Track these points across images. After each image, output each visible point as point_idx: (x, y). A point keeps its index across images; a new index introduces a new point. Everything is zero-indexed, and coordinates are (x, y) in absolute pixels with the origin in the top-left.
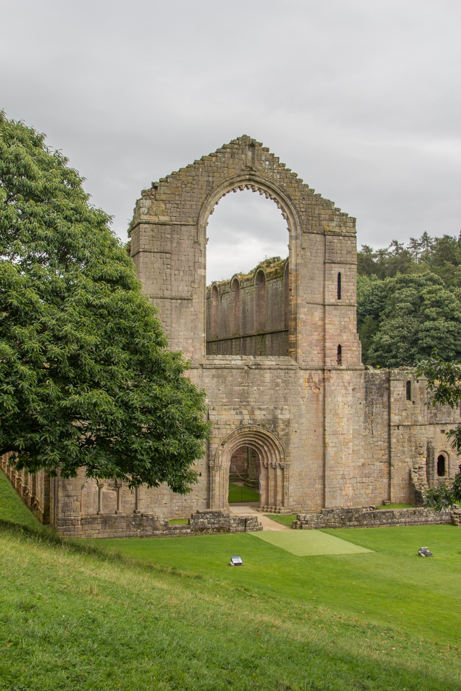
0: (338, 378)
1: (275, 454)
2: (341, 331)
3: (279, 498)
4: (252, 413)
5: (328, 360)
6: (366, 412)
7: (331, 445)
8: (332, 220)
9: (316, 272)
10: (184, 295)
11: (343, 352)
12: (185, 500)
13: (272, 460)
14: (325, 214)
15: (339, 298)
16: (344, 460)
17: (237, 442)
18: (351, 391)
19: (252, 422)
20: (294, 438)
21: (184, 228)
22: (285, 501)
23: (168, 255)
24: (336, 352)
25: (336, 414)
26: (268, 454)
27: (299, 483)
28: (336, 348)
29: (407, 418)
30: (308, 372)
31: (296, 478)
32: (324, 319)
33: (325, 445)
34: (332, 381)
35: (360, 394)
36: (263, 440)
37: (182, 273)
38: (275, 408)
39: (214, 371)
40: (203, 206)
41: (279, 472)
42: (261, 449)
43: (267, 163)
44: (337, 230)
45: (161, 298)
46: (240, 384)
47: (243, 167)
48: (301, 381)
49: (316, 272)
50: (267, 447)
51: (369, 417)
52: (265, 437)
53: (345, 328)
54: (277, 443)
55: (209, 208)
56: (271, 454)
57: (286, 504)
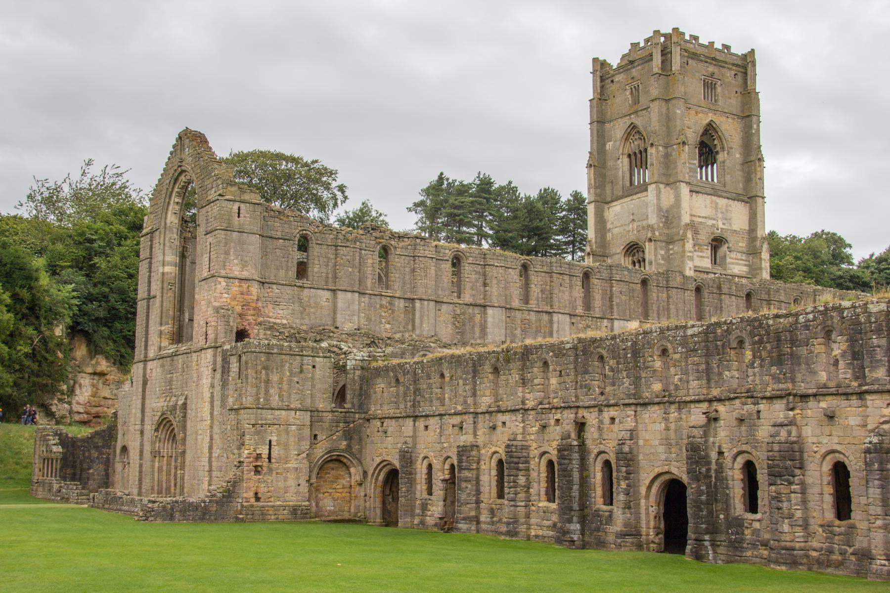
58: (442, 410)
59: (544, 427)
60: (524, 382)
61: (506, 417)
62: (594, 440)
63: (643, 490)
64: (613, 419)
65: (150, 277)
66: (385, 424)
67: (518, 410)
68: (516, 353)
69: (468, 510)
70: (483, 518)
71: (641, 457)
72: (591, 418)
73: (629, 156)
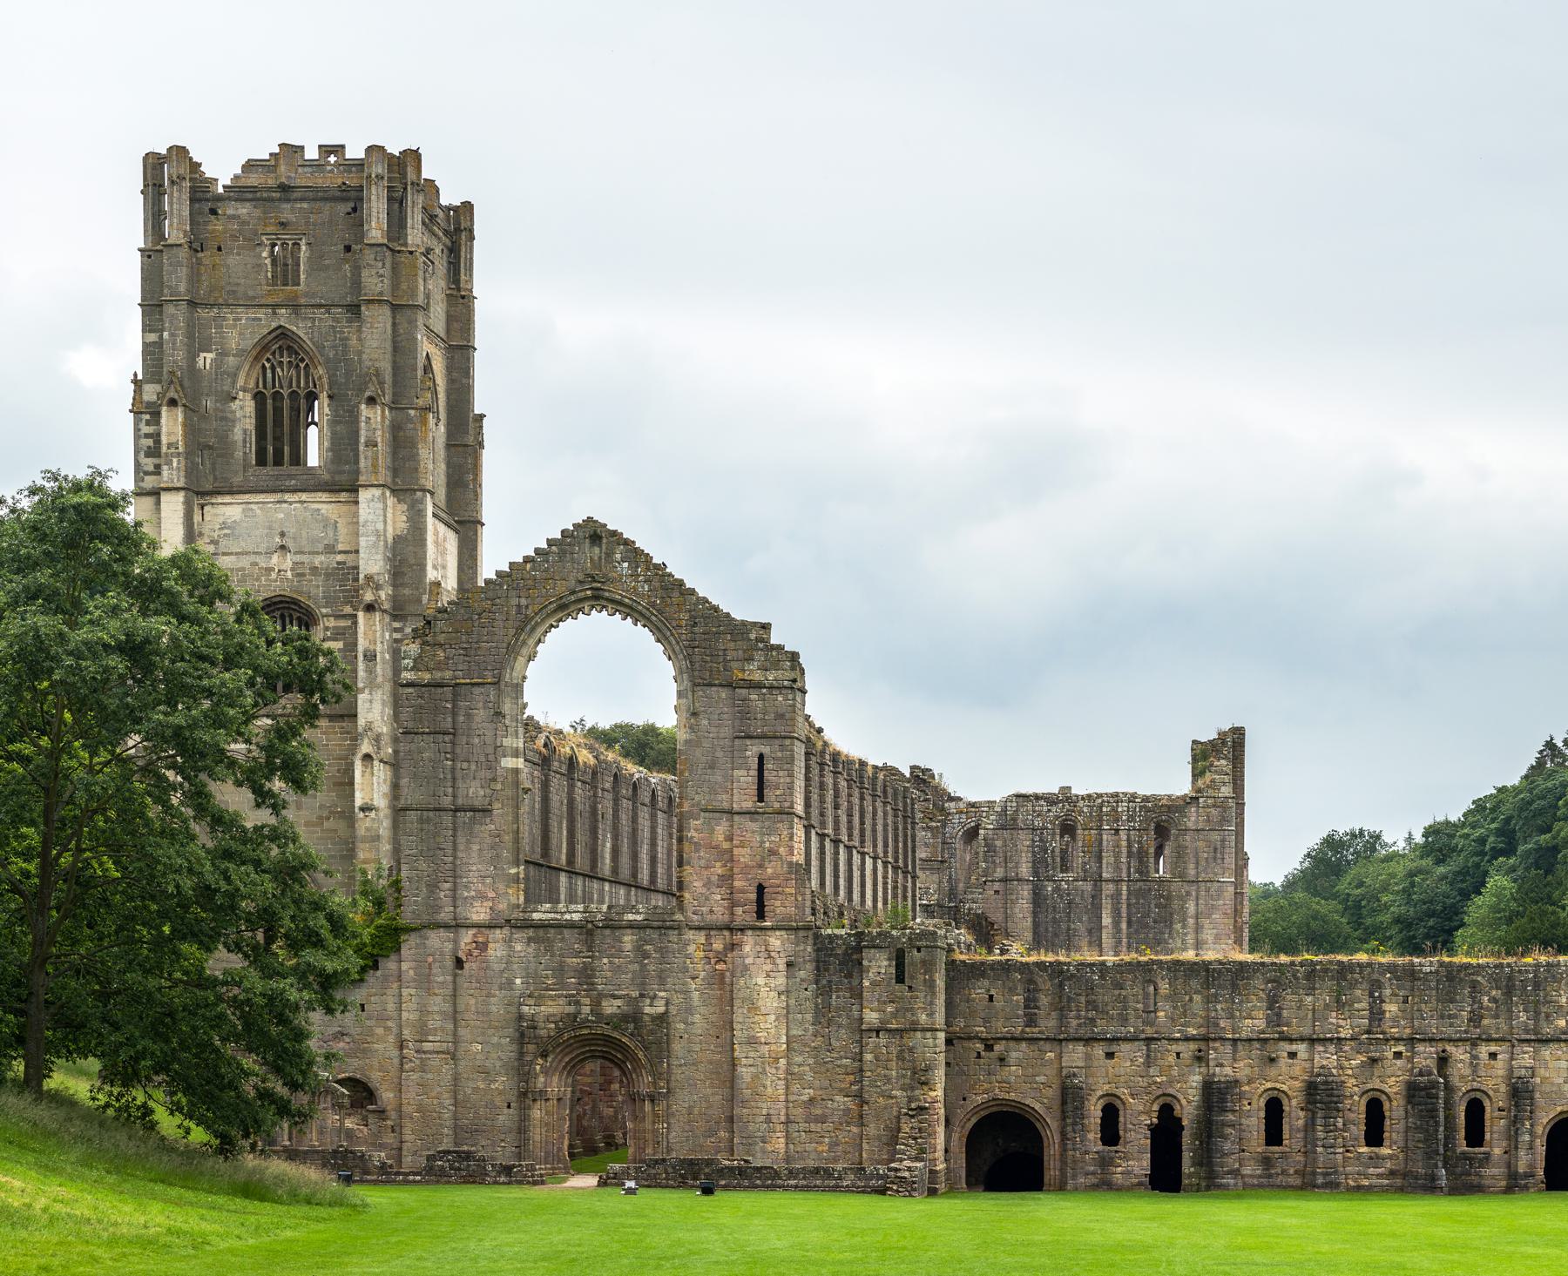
0: (756, 944)
2: (763, 859)
4: (596, 1004)
5: (739, 910)
6: (817, 1005)
7: (744, 1061)
8: (750, 659)
9: (719, 754)
10: (477, 803)
11: (766, 896)
14: (734, 650)
15: (761, 798)
16: (770, 1090)
18: (782, 967)
20: (677, 1047)
21: (477, 690)
23: (447, 738)
24: (753, 896)
25: (754, 1008)
28: (753, 889)
29: (895, 1015)
30: (703, 933)
32: (730, 839)
33: (733, 1064)
34: (747, 949)
35: (805, 973)
37: (473, 767)
38: (642, 996)
39: (531, 932)
40: (512, 650)
43: (626, 565)
44: (758, 676)
45: (435, 809)
46: (577, 954)
47: (581, 577)
48: (691, 948)
49: (719, 754)
51: (823, 1015)
53: (773, 852)
54: (641, 1055)
55: (525, 651)
58: (1149, 1032)
59: (1374, 1061)
60: (1340, 1005)
61: (1301, 1048)
62: (1462, 1077)
63: (1539, 1130)
64: (1493, 1056)
65: (453, 769)
66: (996, 1047)
67: (1331, 1040)
68: (1326, 971)
69: (1232, 1162)
70: (1247, 1171)
71: (1537, 1095)
72: (1459, 1054)
73: (259, 397)
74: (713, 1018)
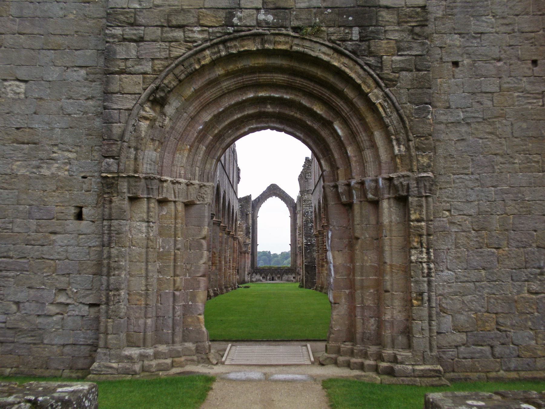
1: (374, 146)
3: (394, 313)
12: (17, 303)
13: (364, 173)
17: (226, 103)
19: (270, 18)
20: (451, 87)
22: (417, 325)
26: (350, 151)
27: (476, 261)
31: (462, 240)
36: (327, 94)
41: (389, 210)
42: (324, 133)
50: (345, 122)
52: (331, 79)
54: (376, 96)
56: (360, 150)
57: (420, 340)
74: (524, 23)
